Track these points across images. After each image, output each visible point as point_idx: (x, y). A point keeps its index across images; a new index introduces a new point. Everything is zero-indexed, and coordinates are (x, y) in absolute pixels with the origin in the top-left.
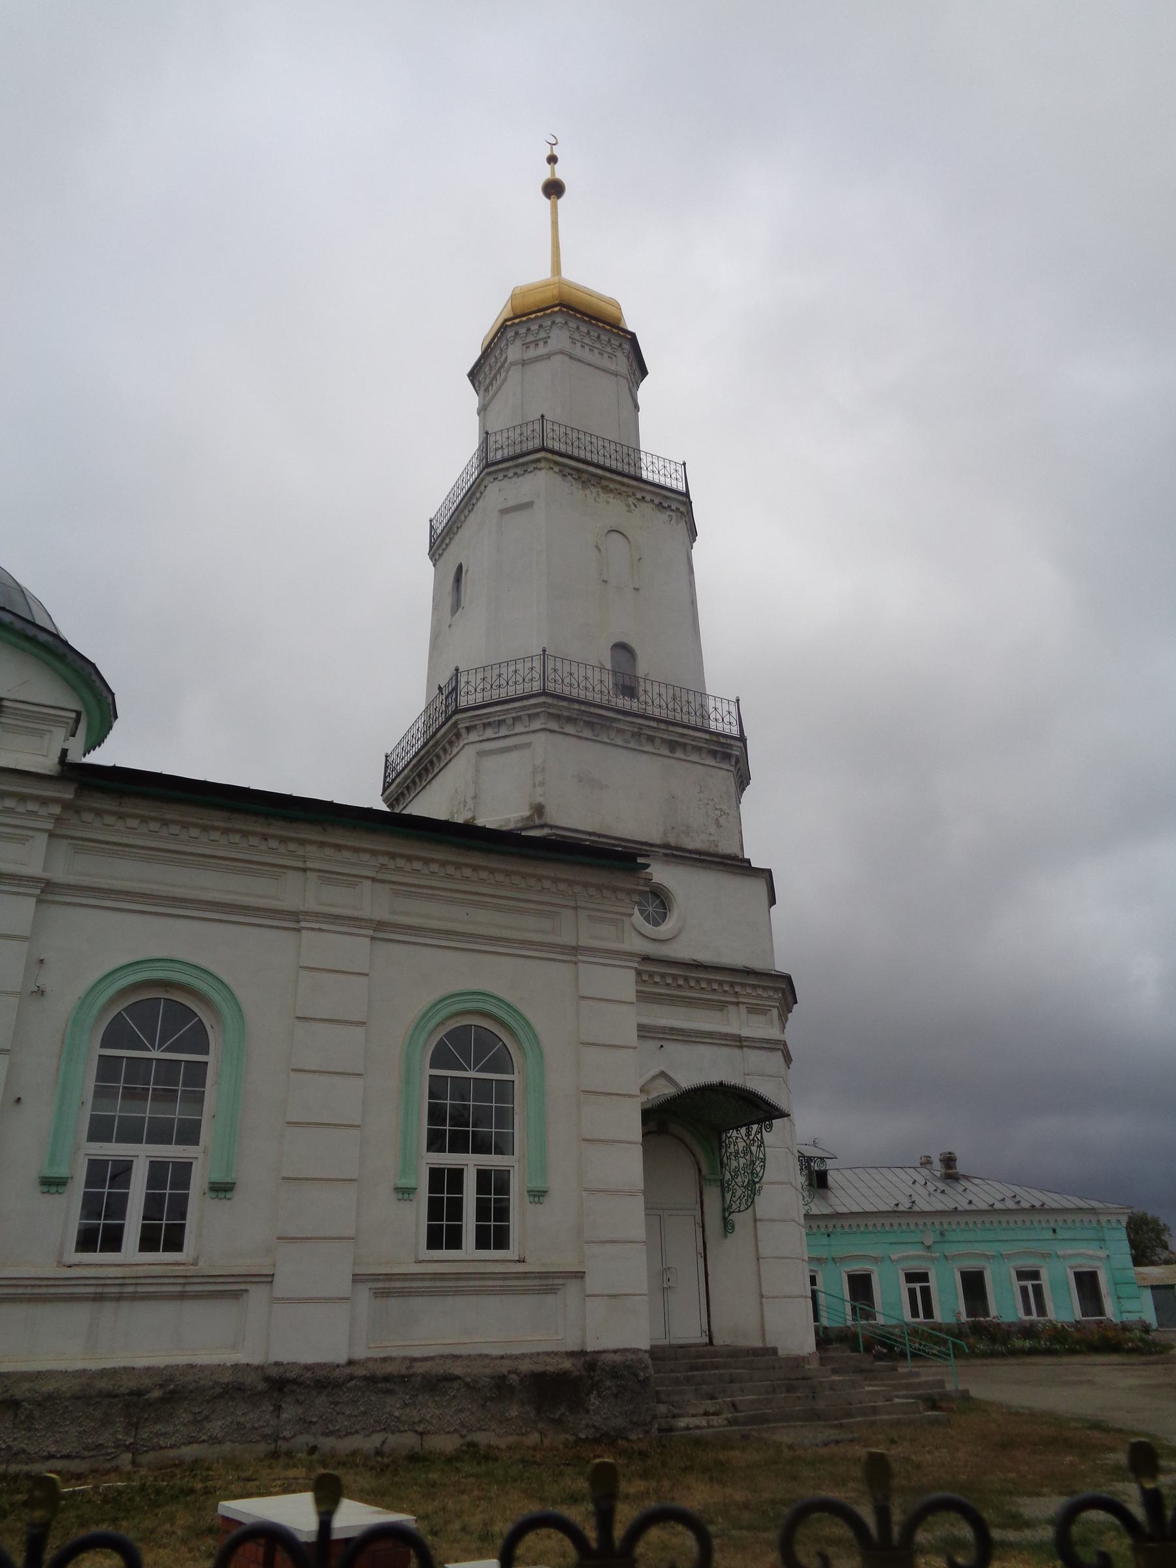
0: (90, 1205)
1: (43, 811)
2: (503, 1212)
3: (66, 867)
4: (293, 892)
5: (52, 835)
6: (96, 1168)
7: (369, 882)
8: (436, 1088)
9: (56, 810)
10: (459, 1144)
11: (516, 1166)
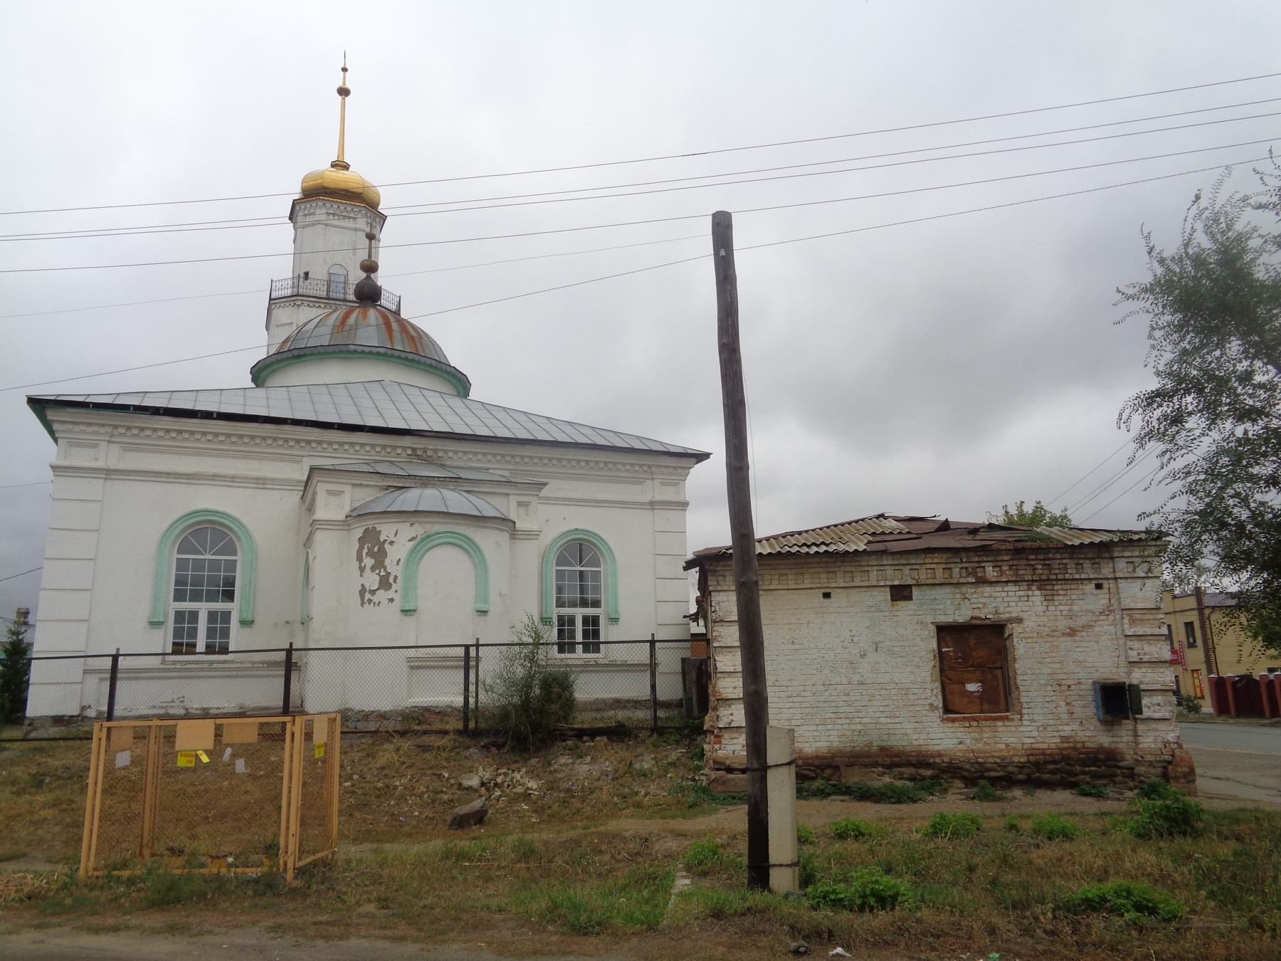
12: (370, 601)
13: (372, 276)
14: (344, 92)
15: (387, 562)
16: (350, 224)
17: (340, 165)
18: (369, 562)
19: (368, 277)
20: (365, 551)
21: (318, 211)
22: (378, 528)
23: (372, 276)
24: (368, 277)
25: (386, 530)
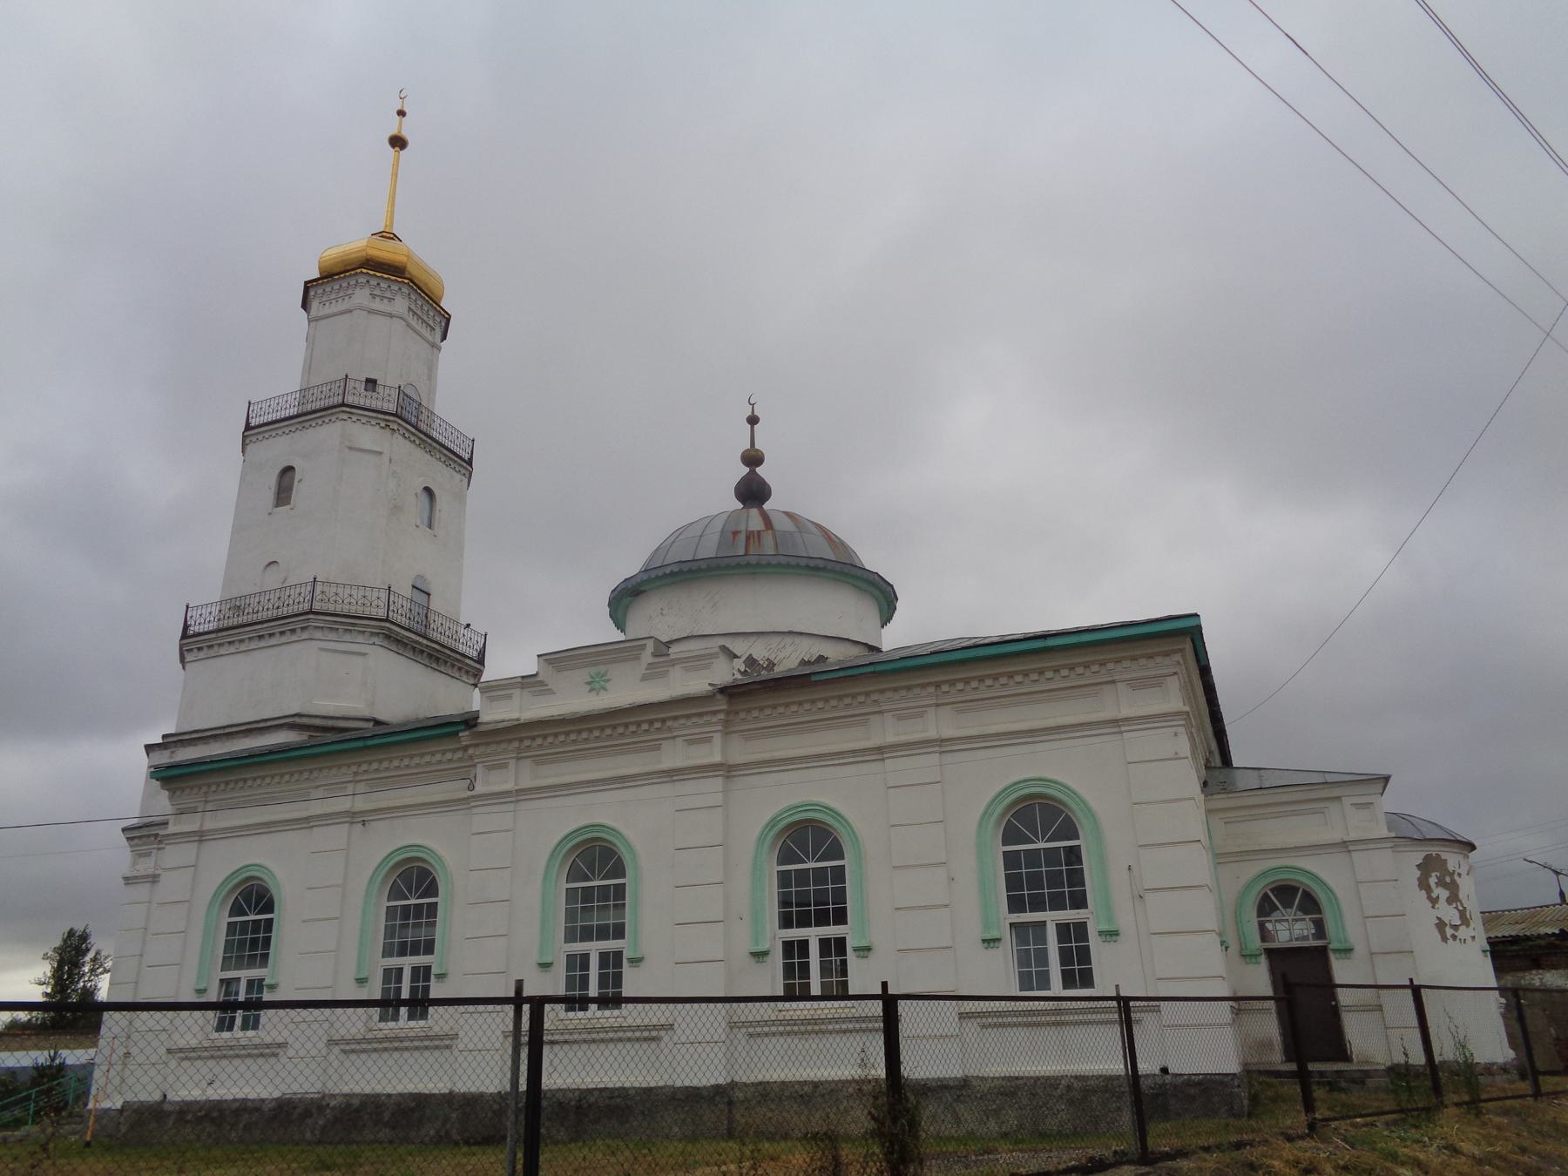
0: (789, 971)
1: (715, 719)
2: (1085, 955)
3: (740, 752)
4: (886, 731)
5: (726, 733)
6: (788, 947)
7: (931, 712)
8: (1011, 860)
9: (722, 716)
10: (1038, 905)
11: (1093, 918)
12: (1454, 937)
13: (759, 470)
14: (398, 142)
15: (1461, 896)
16: (426, 332)
17: (388, 235)
18: (1443, 894)
19: (753, 472)
20: (1433, 881)
21: (398, 298)
22: (1444, 856)
23: (759, 470)
24: (753, 472)
25: (1453, 860)
